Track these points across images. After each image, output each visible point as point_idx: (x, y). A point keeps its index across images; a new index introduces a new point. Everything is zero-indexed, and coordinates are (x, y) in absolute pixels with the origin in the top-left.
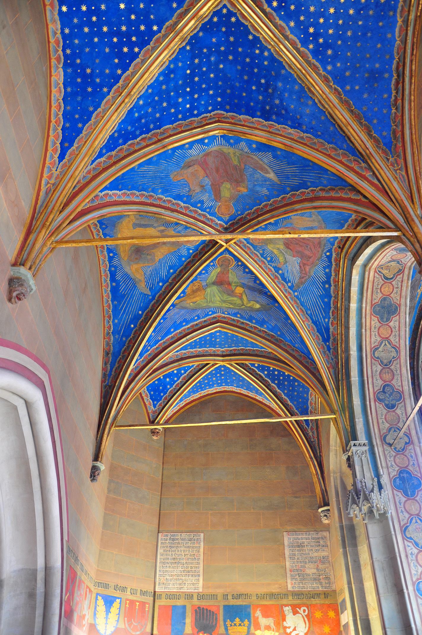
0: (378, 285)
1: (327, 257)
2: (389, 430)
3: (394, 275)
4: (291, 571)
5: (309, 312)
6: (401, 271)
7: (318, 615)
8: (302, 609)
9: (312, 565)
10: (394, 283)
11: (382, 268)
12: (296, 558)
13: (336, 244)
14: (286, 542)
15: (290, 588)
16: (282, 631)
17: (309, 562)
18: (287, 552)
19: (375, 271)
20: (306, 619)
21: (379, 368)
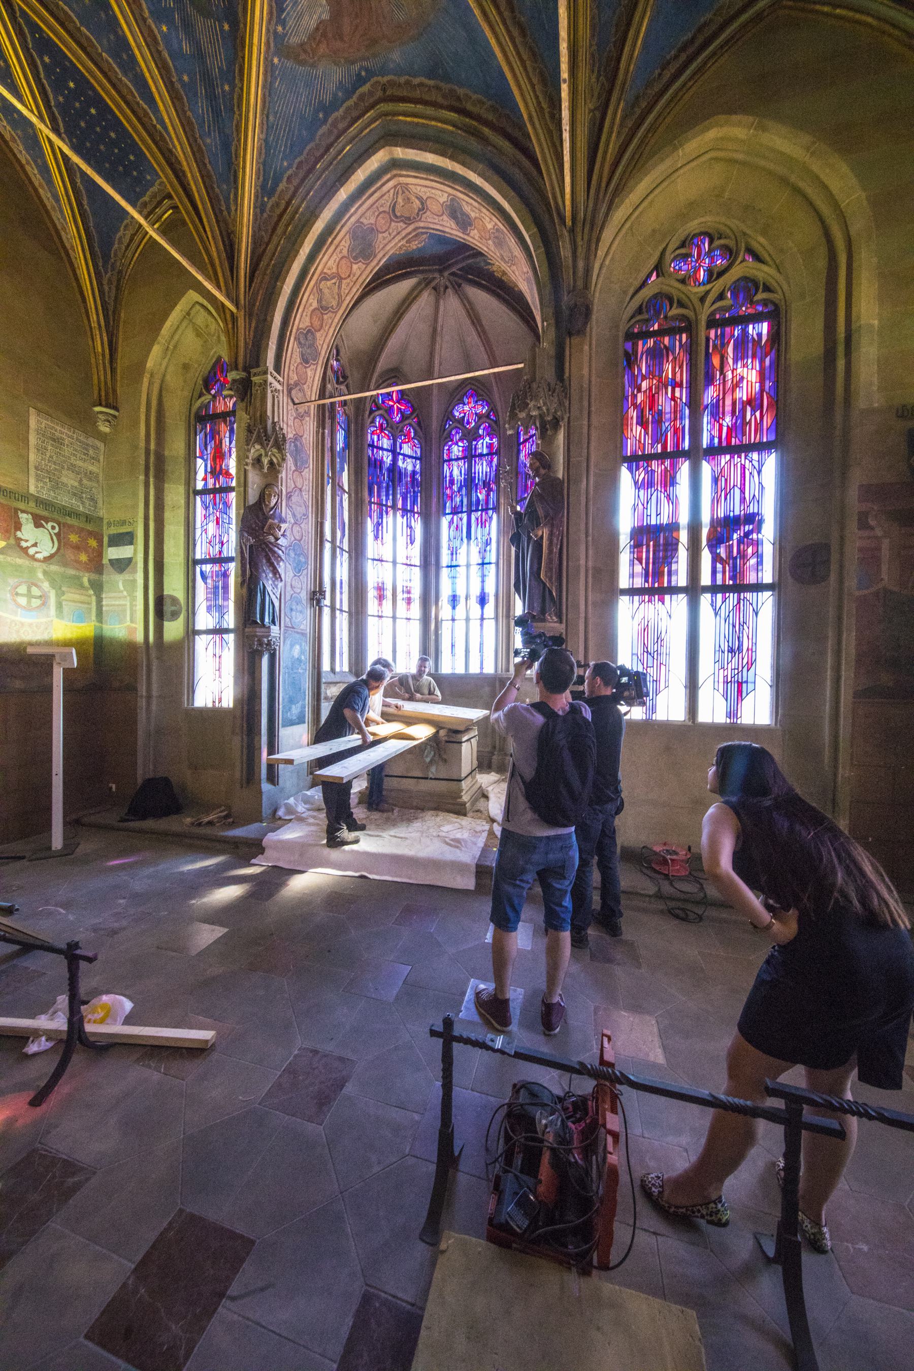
0: (382, 206)
1: (359, 75)
2: (296, 384)
3: (402, 216)
4: (36, 468)
5: (271, 118)
6: (408, 220)
7: (74, 538)
8: (50, 524)
9: (72, 475)
10: (393, 224)
11: (403, 192)
12: (48, 454)
13: (386, 79)
14: (33, 423)
15: (32, 490)
16: (12, 541)
17: (68, 469)
18: (33, 439)
19: (395, 187)
20: (55, 538)
21: (315, 305)
